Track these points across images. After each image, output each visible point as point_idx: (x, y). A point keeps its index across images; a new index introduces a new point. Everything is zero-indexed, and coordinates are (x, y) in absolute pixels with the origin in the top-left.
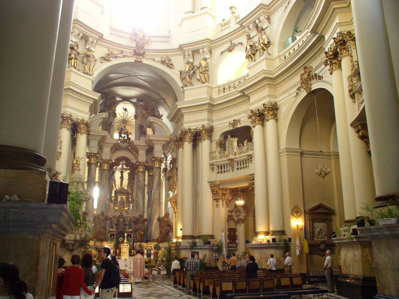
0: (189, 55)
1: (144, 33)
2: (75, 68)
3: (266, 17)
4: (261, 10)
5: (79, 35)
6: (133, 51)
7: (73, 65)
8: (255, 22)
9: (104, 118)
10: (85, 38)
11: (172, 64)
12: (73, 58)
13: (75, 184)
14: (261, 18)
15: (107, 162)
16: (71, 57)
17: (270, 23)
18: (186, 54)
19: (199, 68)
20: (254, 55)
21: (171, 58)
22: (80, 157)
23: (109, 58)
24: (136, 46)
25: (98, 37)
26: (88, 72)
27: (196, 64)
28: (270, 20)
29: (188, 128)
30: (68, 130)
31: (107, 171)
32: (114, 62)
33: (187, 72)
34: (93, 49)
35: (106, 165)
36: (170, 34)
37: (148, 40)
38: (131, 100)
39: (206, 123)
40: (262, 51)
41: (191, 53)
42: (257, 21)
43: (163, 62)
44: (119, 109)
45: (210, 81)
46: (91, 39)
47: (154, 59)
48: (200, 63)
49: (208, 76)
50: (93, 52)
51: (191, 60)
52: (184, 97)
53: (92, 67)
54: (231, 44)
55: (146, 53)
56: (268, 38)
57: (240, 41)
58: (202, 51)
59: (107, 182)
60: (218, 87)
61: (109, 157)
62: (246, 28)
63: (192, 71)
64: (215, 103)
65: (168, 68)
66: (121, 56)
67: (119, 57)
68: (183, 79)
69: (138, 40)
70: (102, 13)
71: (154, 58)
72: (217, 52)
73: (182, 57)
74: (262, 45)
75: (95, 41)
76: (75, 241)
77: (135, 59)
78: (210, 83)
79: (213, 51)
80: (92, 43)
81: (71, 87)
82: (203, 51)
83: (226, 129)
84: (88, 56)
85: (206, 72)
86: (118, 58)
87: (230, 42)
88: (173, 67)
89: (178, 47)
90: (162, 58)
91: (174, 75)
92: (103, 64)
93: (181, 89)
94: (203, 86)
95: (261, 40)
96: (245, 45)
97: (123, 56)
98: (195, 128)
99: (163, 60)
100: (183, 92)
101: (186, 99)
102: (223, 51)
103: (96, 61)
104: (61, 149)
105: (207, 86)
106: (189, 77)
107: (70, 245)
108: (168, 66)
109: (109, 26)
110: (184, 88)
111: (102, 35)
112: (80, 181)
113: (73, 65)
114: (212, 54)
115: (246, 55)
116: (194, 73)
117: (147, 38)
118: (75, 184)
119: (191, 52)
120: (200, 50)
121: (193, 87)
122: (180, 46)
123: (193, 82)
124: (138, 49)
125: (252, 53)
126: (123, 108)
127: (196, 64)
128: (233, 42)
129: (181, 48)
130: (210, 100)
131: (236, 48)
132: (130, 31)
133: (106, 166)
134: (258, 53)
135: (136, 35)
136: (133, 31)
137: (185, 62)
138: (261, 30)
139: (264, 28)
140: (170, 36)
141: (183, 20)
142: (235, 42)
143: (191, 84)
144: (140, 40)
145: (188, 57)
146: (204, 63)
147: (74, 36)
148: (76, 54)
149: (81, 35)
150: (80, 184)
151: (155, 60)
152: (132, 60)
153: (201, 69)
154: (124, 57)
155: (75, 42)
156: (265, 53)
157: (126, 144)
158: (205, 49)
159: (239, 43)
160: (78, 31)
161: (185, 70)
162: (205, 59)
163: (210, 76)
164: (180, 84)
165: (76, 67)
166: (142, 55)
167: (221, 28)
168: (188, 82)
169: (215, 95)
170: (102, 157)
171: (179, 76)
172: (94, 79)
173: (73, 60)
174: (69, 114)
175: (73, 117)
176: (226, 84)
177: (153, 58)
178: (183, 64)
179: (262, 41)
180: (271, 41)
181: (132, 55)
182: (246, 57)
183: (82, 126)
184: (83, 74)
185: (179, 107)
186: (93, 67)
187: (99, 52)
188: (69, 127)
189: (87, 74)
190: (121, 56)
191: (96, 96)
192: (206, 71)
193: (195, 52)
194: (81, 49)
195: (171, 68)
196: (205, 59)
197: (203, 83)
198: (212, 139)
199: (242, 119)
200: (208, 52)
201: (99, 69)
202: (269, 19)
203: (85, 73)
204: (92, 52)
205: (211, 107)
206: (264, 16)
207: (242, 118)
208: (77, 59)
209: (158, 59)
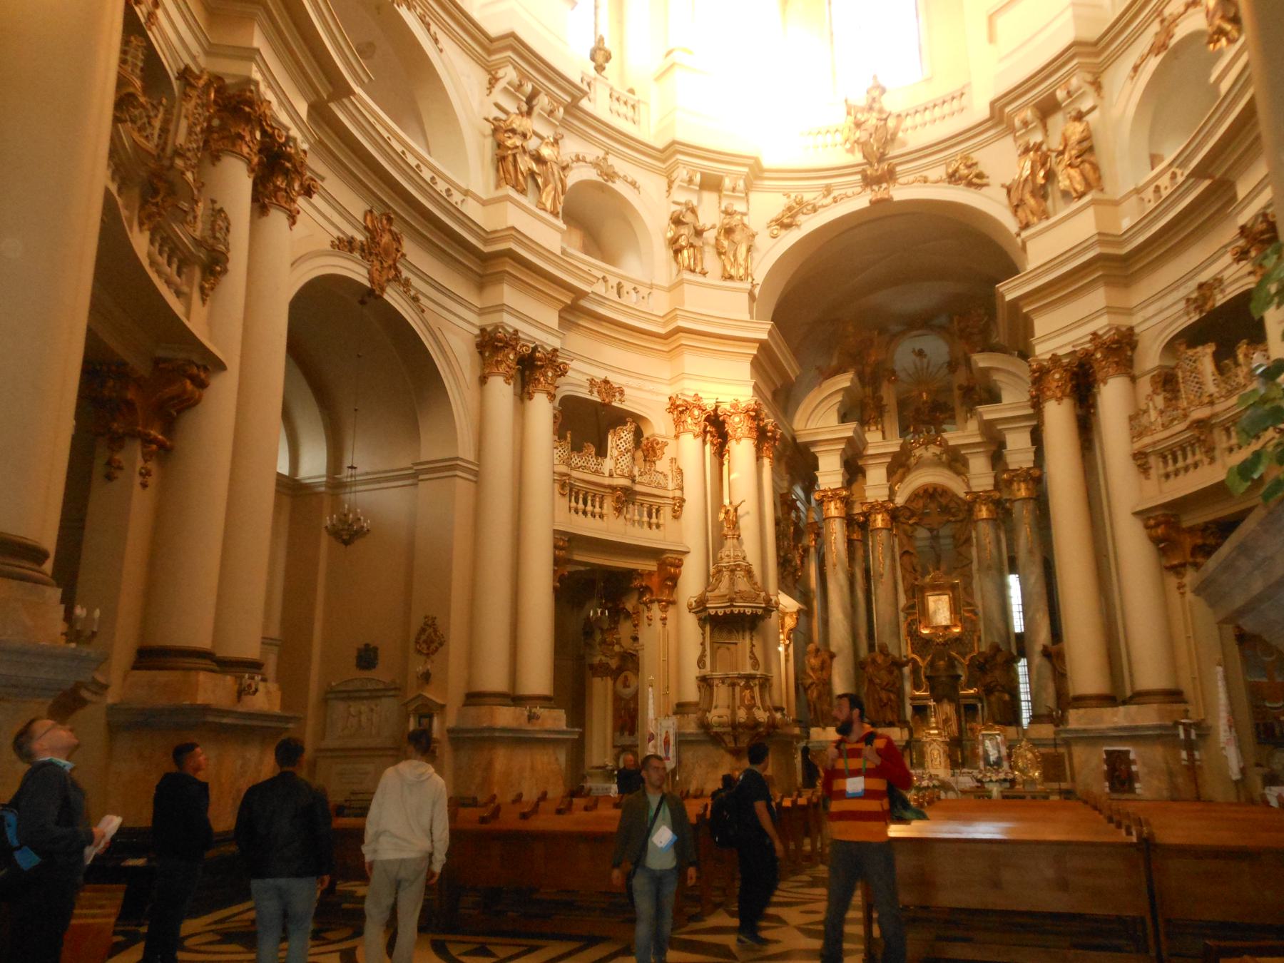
0: (1025, 124)
1: (881, 111)
2: (693, 271)
5: (690, 181)
6: (859, 177)
7: (686, 263)
9: (845, 389)
11: (980, 176)
13: (726, 574)
15: (882, 504)
16: (677, 246)
18: (1017, 123)
19: (1061, 153)
21: (976, 156)
22: (736, 503)
24: (864, 157)
25: (746, 170)
26: (733, 272)
27: (1055, 143)
29: (1049, 356)
30: (695, 436)
31: (884, 532)
32: (809, 224)
33: (1026, 180)
34: (739, 207)
35: (879, 517)
38: (936, 322)
39: (1101, 324)
41: (1028, 114)
43: (953, 178)
44: (903, 356)
45: (1107, 183)
49: (1096, 168)
50: (744, 214)
51: (1037, 137)
55: (898, 169)
58: (1065, 93)
59: (888, 562)
60: (1138, 191)
61: (886, 492)
63: (1042, 173)
65: (972, 189)
66: (825, 202)
67: (823, 206)
68: (1016, 208)
71: (924, 174)
73: (1010, 139)
75: (741, 184)
76: (734, 725)
78: (1107, 189)
80: (734, 190)
83: (1180, 322)
85: (1085, 157)
88: (985, 181)
90: (948, 165)
91: (991, 203)
97: (835, 200)
98: (1069, 349)
99: (950, 171)
100: (1024, 247)
101: (1030, 267)
103: (753, 236)
104: (682, 489)
105: (1094, 202)
106: (1033, 194)
107: (727, 738)
108: (970, 184)
110: (1024, 234)
111: (757, 160)
112: (738, 565)
116: (1050, 176)
118: (726, 574)
122: (992, 104)
124: (870, 164)
126: (914, 351)
130: (1101, 243)
133: (879, 520)
140: (966, 91)
141: (991, 19)
143: (1045, 215)
147: (680, 187)
149: (698, 179)
150: (740, 574)
152: (862, 202)
153: (1066, 156)
155: (686, 204)
157: (934, 450)
158: (1074, 82)
161: (1021, 176)
162: (1080, 117)
163: (1105, 169)
168: (1033, 213)
170: (868, 494)
172: (757, 291)
173: (685, 252)
174: (692, 394)
175: (705, 402)
183: (737, 419)
185: (1008, 298)
188: (697, 430)
189: (731, 278)
191: (762, 330)
193: (1047, 109)
195: (981, 186)
196: (1080, 117)
198: (1136, 372)
200: (1090, 90)
205: (1116, 266)
207: (1221, 271)
208: (692, 246)
209: (939, 172)
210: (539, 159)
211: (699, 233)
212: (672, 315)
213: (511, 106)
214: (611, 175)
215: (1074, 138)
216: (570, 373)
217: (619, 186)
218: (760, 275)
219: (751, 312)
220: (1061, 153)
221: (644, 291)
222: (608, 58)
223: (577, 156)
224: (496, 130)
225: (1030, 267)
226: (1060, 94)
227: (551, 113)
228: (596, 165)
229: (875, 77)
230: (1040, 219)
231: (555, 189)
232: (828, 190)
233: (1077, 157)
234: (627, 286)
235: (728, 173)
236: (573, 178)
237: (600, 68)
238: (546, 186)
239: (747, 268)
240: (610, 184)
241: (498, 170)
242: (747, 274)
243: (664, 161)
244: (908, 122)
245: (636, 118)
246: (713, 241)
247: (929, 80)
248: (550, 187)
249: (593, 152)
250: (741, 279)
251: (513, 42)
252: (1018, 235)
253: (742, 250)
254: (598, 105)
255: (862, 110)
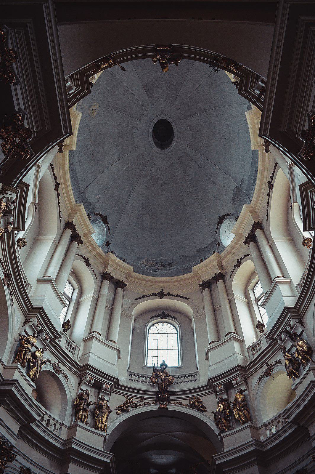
0: (221, 390)
1: (166, 373)
2: (82, 422)
3: (298, 321)
4: (289, 314)
5: (90, 382)
7: (80, 417)
8: (286, 332)
10: (98, 386)
11: (203, 407)
12: (81, 410)
14: (292, 323)
17: (304, 326)
20: (298, 370)
23: (127, 407)
24: (159, 389)
27: (232, 400)
28: (303, 323)
32: (134, 412)
34: (107, 398)
36: (198, 371)
37: (172, 381)
40: (304, 362)
42: (288, 329)
43: (192, 406)
46: (104, 385)
47: (181, 403)
48: (236, 397)
49: (249, 413)
50: (108, 401)
51: (225, 397)
52: (224, 448)
53: (105, 420)
54: (268, 366)
56: (307, 344)
57: (277, 359)
60: (265, 425)
62: (278, 341)
63: (228, 411)
64: (265, 449)
66: (141, 404)
67: (139, 405)
68: (218, 423)
69: (160, 381)
70: (119, 358)
72: (254, 380)
73: (214, 395)
74: (302, 354)
75: (110, 388)
77: (159, 406)
78: (254, 422)
79: (249, 382)
80: (106, 390)
81: (73, 446)
82: (237, 382)
84: (99, 407)
86: (138, 407)
87: (266, 364)
89: (206, 383)
90: (190, 400)
92: (120, 415)
93: (218, 436)
94: (245, 427)
95: (298, 347)
96: (283, 364)
97: (145, 404)
101: (226, 450)
102: (260, 377)
103: (110, 412)
105: (250, 426)
106: (226, 418)
108: (199, 410)
109: (128, 371)
110: (222, 435)
111: (117, 380)
113: (80, 417)
114: (249, 385)
115: (287, 373)
116: (231, 412)
117: (170, 379)
119: (222, 386)
120: (233, 381)
121: (234, 431)
122: (209, 380)
123: (231, 425)
124: (161, 393)
125: (294, 368)
127: (232, 400)
128: (269, 363)
129: (211, 382)
131: (274, 369)
132: (150, 373)
134: (301, 367)
135: (157, 376)
136: (154, 373)
137: (218, 401)
138: (294, 337)
139: (298, 334)
140: (197, 374)
142: (271, 362)
144: (162, 381)
145: (220, 393)
146: (240, 397)
148: (84, 404)
151: (184, 404)
152: (155, 407)
153: (238, 405)
154: (145, 405)
156: (309, 364)
158: (238, 379)
159: (276, 363)
160: (88, 378)
161: (219, 410)
162: (241, 392)
163: (251, 412)
164: (216, 430)
165: (84, 420)
166: (168, 400)
167: (252, 352)
169: (262, 438)
171: (214, 420)
176: (273, 420)
177: (180, 402)
178: (217, 403)
179: (300, 349)
180: (312, 346)
181: (155, 402)
182: (288, 375)
184: (93, 430)
185: (218, 462)
186: (106, 419)
187: (115, 401)
189: (97, 428)
190: (142, 403)
192: (245, 406)
193: (228, 387)
194: (92, 399)
195: (203, 411)
196: (241, 392)
197: (244, 423)
199: (308, 468)
200: (244, 383)
201: (113, 421)
202: (301, 322)
203: (95, 429)
204: (106, 402)
206: (294, 320)
210: (34, 356)
211: (88, 404)
212: (69, 441)
213: (30, 333)
214: (58, 371)
215: (240, 400)
216: (14, 462)
217: (60, 376)
218: (110, 430)
219: (103, 448)
220: (235, 405)
221: (58, 426)
222: (69, 328)
223: (48, 360)
224: (21, 340)
225: (226, 450)
226: (234, 382)
227: (44, 340)
228: (54, 365)
229: (163, 361)
230: (228, 430)
231: (37, 370)
232: (143, 399)
233: (242, 407)
234: (52, 422)
235: (106, 383)
236: (44, 367)
237: (65, 330)
238: (33, 367)
239: (105, 426)
240: (57, 374)
241: (16, 356)
242: (105, 429)
243: (80, 371)
244: (175, 380)
245: (74, 352)
246: (92, 410)
247: (181, 367)
248: (35, 368)
249: (54, 360)
250: (102, 431)
251: (41, 310)
252: (219, 435)
253: (105, 417)
254: (62, 343)
255: (159, 371)
